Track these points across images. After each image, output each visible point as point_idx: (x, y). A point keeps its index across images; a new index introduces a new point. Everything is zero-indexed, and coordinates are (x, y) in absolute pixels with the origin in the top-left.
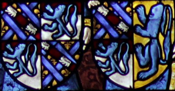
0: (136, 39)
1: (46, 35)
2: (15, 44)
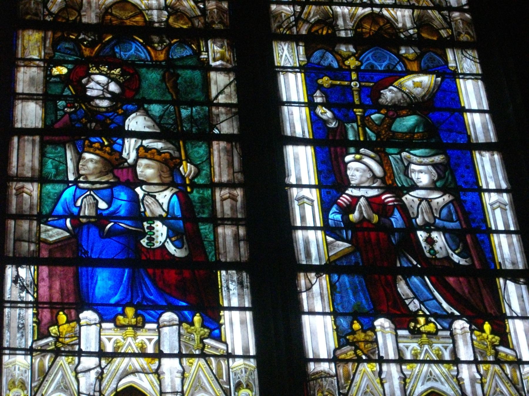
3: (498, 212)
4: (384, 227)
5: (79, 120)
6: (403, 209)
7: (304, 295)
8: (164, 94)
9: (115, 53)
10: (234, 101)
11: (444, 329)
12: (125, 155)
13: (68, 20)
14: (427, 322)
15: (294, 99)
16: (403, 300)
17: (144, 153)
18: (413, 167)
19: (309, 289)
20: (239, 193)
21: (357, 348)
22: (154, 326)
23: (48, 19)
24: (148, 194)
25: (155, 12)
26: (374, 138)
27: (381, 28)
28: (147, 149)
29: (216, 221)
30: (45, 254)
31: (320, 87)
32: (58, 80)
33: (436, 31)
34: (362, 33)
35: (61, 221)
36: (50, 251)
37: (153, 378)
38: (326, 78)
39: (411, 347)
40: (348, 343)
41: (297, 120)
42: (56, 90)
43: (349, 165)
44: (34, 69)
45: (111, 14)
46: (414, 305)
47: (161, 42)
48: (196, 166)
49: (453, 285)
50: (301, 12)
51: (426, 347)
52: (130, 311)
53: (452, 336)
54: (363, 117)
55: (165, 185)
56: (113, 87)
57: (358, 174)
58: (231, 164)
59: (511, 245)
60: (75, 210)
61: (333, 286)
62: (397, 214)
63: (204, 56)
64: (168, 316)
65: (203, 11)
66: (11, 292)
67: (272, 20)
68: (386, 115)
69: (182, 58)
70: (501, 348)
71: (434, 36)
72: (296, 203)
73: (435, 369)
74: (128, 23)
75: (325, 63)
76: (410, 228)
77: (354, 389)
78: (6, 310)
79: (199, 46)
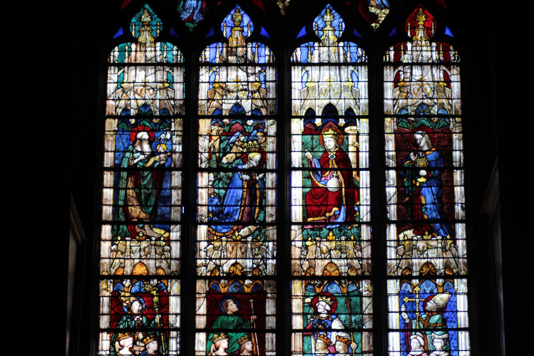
5: (315, 324)
8: (345, 310)
9: (328, 290)
10: (371, 312)
12: (331, 340)
13: (310, 274)
15: (394, 310)
18: (435, 340)
23: (303, 274)
25: (343, 267)
26: (422, 327)
27: (430, 270)
28: (340, 337)
31: (404, 302)
32: (307, 305)
33: (451, 270)
34: (422, 273)
38: (407, 298)
41: (394, 321)
42: (307, 310)
43: (412, 341)
44: (299, 300)
45: (326, 270)
47: (345, 283)
48: (357, 344)
50: (399, 264)
54: (419, 317)
56: (328, 308)
57: (415, 345)
58: (369, 343)
63: (361, 290)
65: (361, 265)
67: (388, 268)
68: (428, 315)
69: (353, 291)
71: (450, 272)
74: (333, 274)
75: (407, 290)
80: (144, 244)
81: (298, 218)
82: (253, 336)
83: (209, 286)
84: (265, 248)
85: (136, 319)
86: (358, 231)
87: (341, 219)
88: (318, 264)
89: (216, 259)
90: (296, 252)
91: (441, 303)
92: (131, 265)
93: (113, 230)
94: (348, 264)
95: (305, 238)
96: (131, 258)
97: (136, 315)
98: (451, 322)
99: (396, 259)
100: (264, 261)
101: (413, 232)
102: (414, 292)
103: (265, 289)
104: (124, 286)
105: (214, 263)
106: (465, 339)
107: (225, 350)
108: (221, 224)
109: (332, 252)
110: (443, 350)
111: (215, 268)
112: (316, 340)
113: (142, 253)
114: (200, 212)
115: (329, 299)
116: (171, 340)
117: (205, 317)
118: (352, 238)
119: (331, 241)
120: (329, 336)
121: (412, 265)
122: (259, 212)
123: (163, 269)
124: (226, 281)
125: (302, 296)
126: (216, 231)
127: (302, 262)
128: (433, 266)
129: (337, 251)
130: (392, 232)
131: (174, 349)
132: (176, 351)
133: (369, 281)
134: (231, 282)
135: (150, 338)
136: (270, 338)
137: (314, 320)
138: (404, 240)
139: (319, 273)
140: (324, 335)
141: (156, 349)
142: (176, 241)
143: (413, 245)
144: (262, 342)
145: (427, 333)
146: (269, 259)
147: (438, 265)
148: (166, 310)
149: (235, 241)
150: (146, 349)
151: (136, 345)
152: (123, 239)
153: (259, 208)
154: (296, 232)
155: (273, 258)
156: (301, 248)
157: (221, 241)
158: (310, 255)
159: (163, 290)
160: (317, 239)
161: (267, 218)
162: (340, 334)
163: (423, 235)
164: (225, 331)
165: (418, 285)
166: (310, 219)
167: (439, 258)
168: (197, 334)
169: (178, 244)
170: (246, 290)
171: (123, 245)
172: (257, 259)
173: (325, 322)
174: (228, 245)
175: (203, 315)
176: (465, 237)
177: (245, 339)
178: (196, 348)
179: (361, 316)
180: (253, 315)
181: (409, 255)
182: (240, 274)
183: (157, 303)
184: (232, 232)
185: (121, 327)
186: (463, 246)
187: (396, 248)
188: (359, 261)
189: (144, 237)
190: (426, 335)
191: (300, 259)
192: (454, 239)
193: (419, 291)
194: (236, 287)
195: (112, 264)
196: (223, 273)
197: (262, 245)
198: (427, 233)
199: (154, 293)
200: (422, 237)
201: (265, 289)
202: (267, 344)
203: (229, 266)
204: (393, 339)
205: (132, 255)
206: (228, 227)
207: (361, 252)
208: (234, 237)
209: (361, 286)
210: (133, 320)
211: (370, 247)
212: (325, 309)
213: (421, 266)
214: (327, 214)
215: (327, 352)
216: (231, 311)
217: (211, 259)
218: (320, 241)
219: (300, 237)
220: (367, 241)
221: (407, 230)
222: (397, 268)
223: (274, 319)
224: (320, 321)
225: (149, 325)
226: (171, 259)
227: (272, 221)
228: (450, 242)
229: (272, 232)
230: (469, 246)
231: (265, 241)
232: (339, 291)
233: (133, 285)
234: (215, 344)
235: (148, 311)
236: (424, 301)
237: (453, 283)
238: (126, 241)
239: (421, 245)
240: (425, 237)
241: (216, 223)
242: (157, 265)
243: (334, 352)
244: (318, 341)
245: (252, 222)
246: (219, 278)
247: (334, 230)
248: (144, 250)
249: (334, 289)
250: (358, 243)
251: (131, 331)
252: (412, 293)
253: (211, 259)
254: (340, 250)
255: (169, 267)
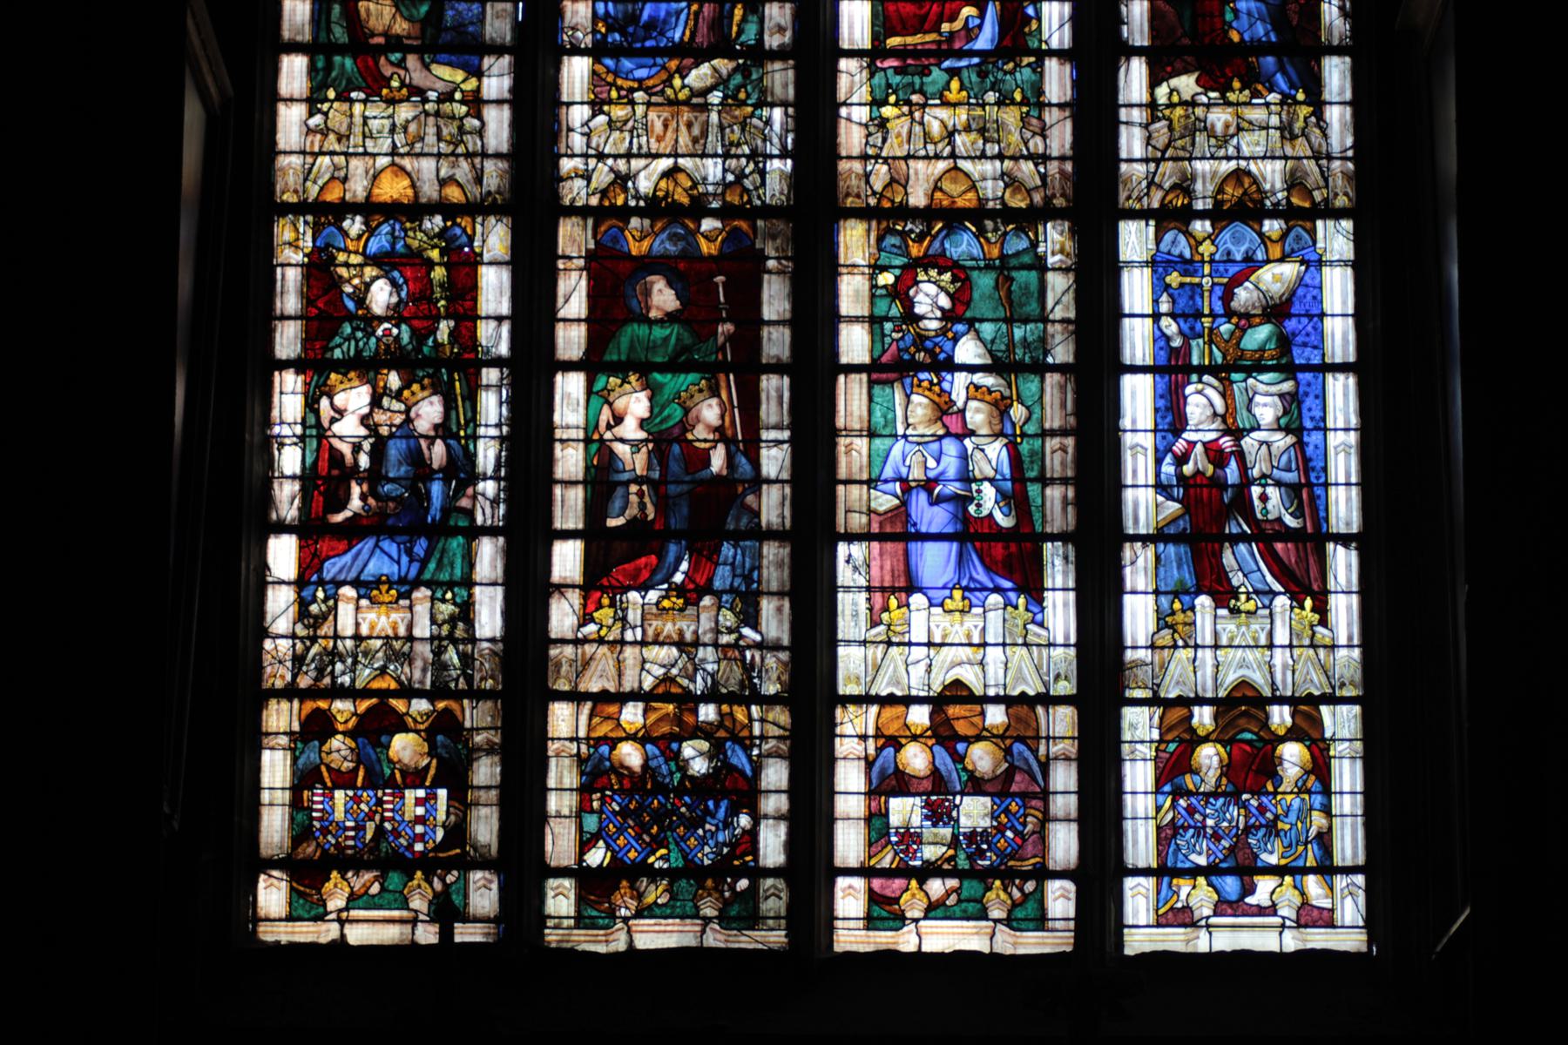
0: (1280, 825)
1: (1210, 822)
2: (1186, 829)
3: (1341, 456)
4: (1218, 483)
5: (906, 350)
6: (1240, 455)
7: (1128, 571)
9: (944, 250)
10: (1072, 315)
11: (1264, 607)
12: (954, 397)
13: (893, 202)
14: (1248, 599)
16: (1226, 573)
17: (975, 390)
18: (1258, 398)
19: (1133, 563)
20: (1070, 442)
21: (1175, 631)
22: (980, 610)
23: (872, 201)
24: (977, 447)
25: (990, 183)
27: (1245, 193)
28: (977, 388)
29: (1044, 481)
30: (875, 528)
31: (1168, 287)
32: (884, 292)
33: (1308, 194)
35: (889, 486)
36: (881, 524)
37: (978, 669)
38: (1175, 274)
39: (1228, 628)
40: (1167, 626)
41: (1137, 341)
42: (882, 307)
43: (1189, 400)
44: (859, 278)
45: (941, 190)
46: (1237, 579)
47: (996, 230)
48: (1028, 408)
49: (1281, 553)
50: (1155, 174)
51: (1243, 629)
52: (957, 594)
53: (1271, 615)
54: (1211, 330)
55: (996, 435)
56: (944, 301)
57: (1198, 411)
58: (1063, 405)
59: (1348, 499)
60: (904, 471)
61: (1158, 558)
62: (1233, 464)
63: (1041, 249)
64: (995, 599)
65: (1043, 177)
66: (844, 574)
67: (1121, 187)
68: (1237, 325)
69: (1018, 254)
70: (1320, 629)
71: (1304, 200)
72: (1129, 453)
73: (1250, 655)
74: (960, 203)
75: (1176, 252)
76: (1246, 482)
77: (1168, 678)
78: (840, 595)
79: (1036, 235)
80: (405, 112)
81: (857, 35)
82: (723, 384)
83: (594, 236)
84: (761, 124)
85: (379, 332)
86: (1033, 77)
87: (984, 42)
88: (916, 173)
89: (616, 157)
90: (851, 138)
91: (1277, 289)
92: (367, 172)
93: (312, 70)
94: (1003, 174)
95: (879, 95)
96: (366, 154)
97: (381, 320)
98: (1305, 345)
99: (1146, 160)
100: (756, 164)
101: (1198, 82)
102: (1197, 258)
103: (758, 245)
104: (345, 234)
105: (611, 169)
106: (1346, 395)
107: (642, 423)
108: (630, 53)
109: (958, 139)
110: (1280, 429)
111: (612, 183)
112: (908, 397)
113: (400, 139)
114: (569, 19)
115: (947, 276)
116: (484, 394)
117: (583, 328)
118: (1018, 97)
119: (955, 105)
120: (946, 386)
121: (1193, 179)
122: (744, 20)
123: (459, 185)
124: (647, 222)
125: (869, 266)
126: (616, 74)
127: (869, 168)
128: (1255, 181)
129: (974, 135)
130: (1134, 79)
131: (493, 419)
132: (499, 425)
133: (1067, 224)
134: (659, 225)
135: (423, 388)
136: (774, 388)
137: (902, 338)
138: (1171, 105)
139: (918, 199)
140: (931, 383)
141: (438, 419)
142: (499, 102)
143: (1197, 119)
144: (750, 402)
145: (1235, 376)
146: (772, 157)
147: (1269, 178)
148: (468, 304)
149: (673, 103)
150: (408, 420)
151: (380, 407)
152: (343, 97)
153: (744, 8)
154: (851, 78)
155: (783, 155)
156: (866, 126)
157: (632, 103)
158: (894, 148)
159: (461, 247)
160: (915, 98)
161: (766, 37)
162: (979, 378)
163: (1224, 88)
164: (641, 368)
165: (1209, 237)
166: (894, 42)
167: (1273, 158)
168: (559, 377)
169: (506, 112)
170: (706, 247)
171: (344, 113)
172: (738, 157)
173: (936, 344)
174: (652, 115)
175: (579, 320)
176: (1348, 96)
177: (701, 391)
178: (557, 418)
179: (1041, 326)
180: (724, 321)
181: (1183, 148)
182: (685, 200)
183: (441, 285)
184: (664, 76)
185: (338, 354)
186: (1343, 124)
187: (1146, 126)
188: (1036, 165)
189: (404, 91)
190: (1232, 382)
191: (864, 157)
192: (1318, 104)
193: (1212, 255)
194: (673, 238)
195: (310, 170)
196: (637, 197)
197: (752, 115)
198: (1236, 84)
199: (435, 254)
200: (1223, 96)
201: (758, 245)
202: (764, 407)
203: (655, 178)
204: (1133, 394)
205: (369, 143)
206: (651, 62)
207: (1044, 137)
208: (669, 91)
209: (1041, 238)
210: (373, 333)
211: (1068, 125)
212: (935, 304)
213: (1218, 180)
214: (945, 27)
215: (941, 432)
216: (658, 308)
217: (601, 157)
218: (924, 106)
219: (863, 94)
220: (1061, 106)
221: (1178, 74)
222: (1148, 187)
223: (786, 333)
224: (921, 340)
225: (418, 349)
226: (484, 155)
227: (781, 46)
228: (1304, 111)
229: (781, 78)
230: (1360, 125)
231: (760, 104)
232: (976, 251)
233: (371, 231)
234: (611, 405)
235: (416, 309)
236: (1225, 285)
237: (1312, 233)
238: (352, 101)
239: (1219, 118)
240: (1232, 97)
241: (617, 52)
242: (443, 173)
243: (959, 431)
244: (914, 398)
245: (721, 46)
246: (625, 213)
247: (965, 74)
248: (405, 128)
249: (963, 246)
250: (1034, 113)
251: (365, 367)
252: (1191, 261)
253: (601, 157)
254: (982, 131)
255: (479, 180)
